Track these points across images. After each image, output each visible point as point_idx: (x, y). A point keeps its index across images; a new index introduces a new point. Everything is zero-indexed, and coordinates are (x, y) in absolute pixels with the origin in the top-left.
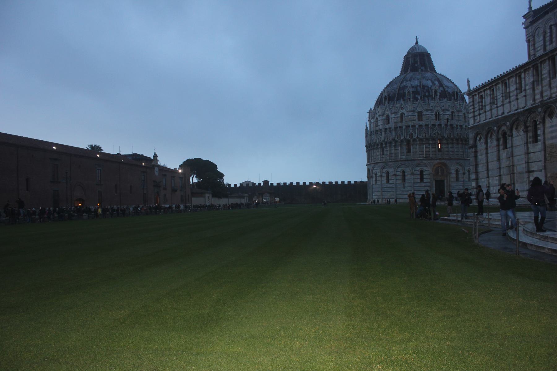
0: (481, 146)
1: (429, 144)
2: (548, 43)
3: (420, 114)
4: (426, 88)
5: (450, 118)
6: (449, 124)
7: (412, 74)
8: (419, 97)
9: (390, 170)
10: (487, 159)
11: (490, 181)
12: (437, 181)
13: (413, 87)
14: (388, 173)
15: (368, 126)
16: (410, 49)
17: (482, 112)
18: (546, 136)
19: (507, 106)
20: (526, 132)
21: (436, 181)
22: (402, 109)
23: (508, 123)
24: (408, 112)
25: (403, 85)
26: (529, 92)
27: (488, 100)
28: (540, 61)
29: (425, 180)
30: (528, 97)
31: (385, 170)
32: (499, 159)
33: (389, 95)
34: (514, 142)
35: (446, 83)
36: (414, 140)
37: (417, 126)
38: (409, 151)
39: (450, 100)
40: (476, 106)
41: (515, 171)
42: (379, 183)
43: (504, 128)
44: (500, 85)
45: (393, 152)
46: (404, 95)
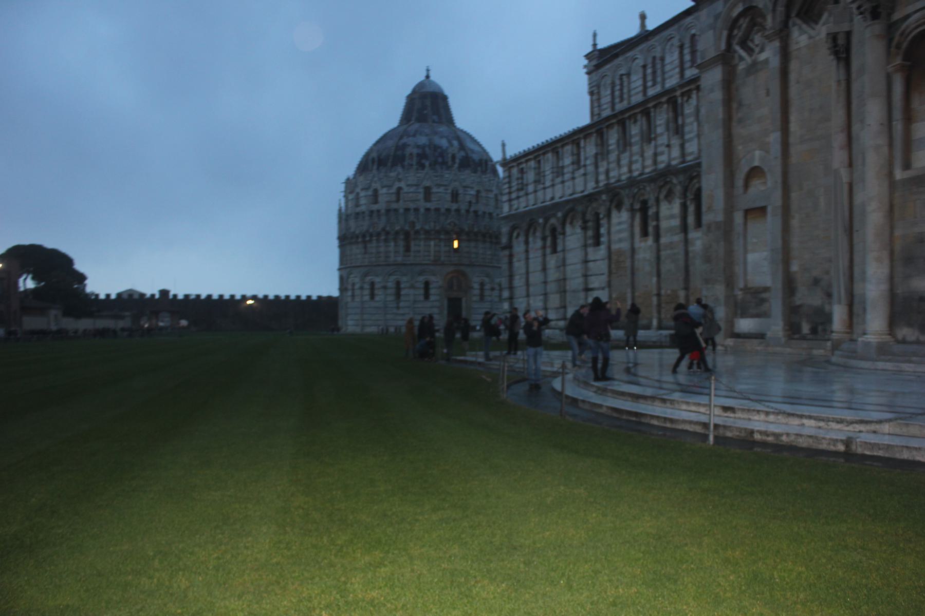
0: (519, 248)
2: (617, 100)
3: (428, 191)
4: (439, 150)
5: (474, 201)
6: (472, 209)
7: (417, 125)
8: (427, 164)
9: (377, 280)
10: (527, 268)
11: (531, 302)
12: (450, 300)
13: (418, 147)
14: (372, 284)
15: (343, 205)
17: (522, 193)
19: (559, 187)
20: (585, 228)
22: (400, 180)
23: (560, 214)
24: (408, 185)
26: (591, 169)
27: (531, 176)
28: (607, 124)
29: (432, 298)
30: (588, 177)
31: (368, 279)
32: (544, 269)
33: (379, 157)
34: (567, 243)
36: (417, 232)
37: (422, 210)
38: (408, 249)
39: (475, 172)
42: (357, 299)
43: (553, 221)
44: (550, 155)
45: (382, 249)
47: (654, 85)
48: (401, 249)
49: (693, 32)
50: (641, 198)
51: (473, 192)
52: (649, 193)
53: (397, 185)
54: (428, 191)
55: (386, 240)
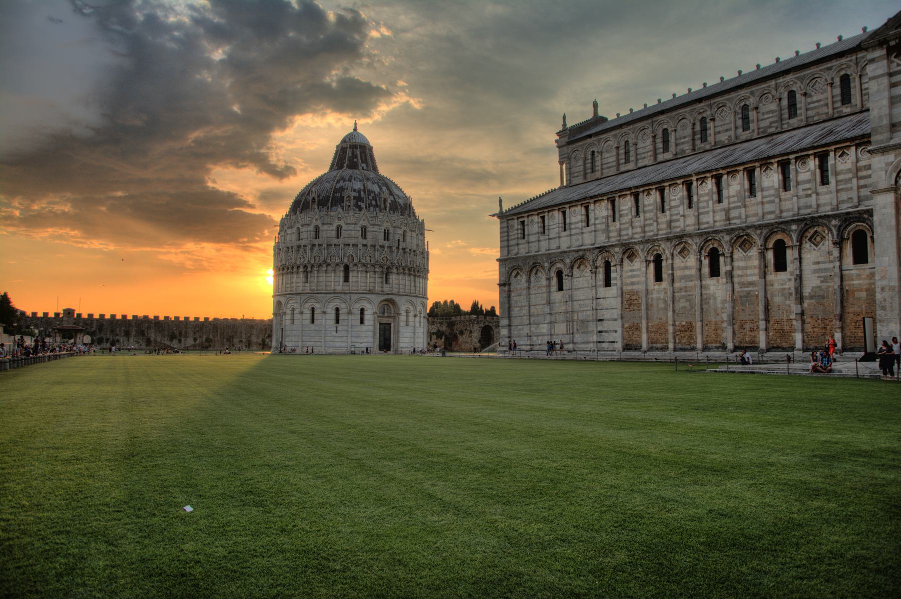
1: (375, 272)
3: (364, 231)
7: (350, 171)
9: (317, 306)
13: (354, 190)
16: (347, 136)
18: (624, 281)
21: (381, 324)
22: (339, 219)
23: (568, 261)
24: (347, 224)
25: (339, 186)
29: (366, 322)
31: (308, 306)
33: (319, 196)
35: (396, 191)
36: (355, 265)
37: (360, 246)
38: (346, 279)
40: (511, 234)
41: (576, 318)
46: (342, 200)
47: (627, 161)
48: (342, 279)
49: (665, 127)
50: (655, 253)
51: (401, 232)
52: (666, 249)
53: (337, 223)
54: (364, 231)
55: (326, 271)
